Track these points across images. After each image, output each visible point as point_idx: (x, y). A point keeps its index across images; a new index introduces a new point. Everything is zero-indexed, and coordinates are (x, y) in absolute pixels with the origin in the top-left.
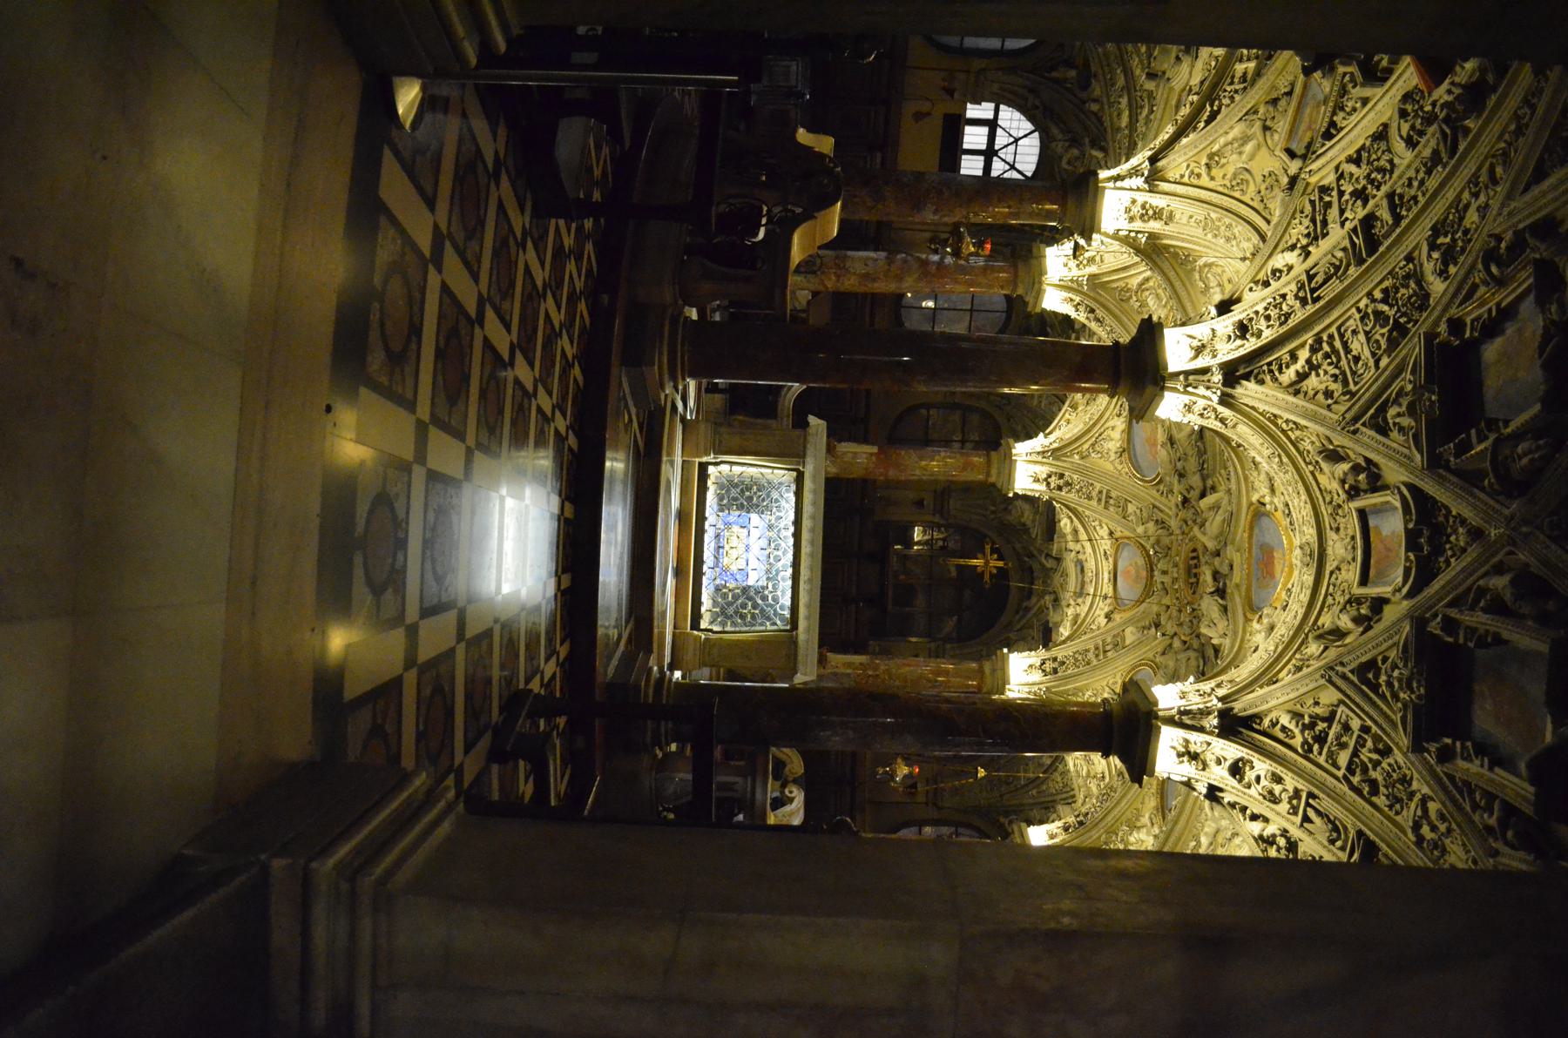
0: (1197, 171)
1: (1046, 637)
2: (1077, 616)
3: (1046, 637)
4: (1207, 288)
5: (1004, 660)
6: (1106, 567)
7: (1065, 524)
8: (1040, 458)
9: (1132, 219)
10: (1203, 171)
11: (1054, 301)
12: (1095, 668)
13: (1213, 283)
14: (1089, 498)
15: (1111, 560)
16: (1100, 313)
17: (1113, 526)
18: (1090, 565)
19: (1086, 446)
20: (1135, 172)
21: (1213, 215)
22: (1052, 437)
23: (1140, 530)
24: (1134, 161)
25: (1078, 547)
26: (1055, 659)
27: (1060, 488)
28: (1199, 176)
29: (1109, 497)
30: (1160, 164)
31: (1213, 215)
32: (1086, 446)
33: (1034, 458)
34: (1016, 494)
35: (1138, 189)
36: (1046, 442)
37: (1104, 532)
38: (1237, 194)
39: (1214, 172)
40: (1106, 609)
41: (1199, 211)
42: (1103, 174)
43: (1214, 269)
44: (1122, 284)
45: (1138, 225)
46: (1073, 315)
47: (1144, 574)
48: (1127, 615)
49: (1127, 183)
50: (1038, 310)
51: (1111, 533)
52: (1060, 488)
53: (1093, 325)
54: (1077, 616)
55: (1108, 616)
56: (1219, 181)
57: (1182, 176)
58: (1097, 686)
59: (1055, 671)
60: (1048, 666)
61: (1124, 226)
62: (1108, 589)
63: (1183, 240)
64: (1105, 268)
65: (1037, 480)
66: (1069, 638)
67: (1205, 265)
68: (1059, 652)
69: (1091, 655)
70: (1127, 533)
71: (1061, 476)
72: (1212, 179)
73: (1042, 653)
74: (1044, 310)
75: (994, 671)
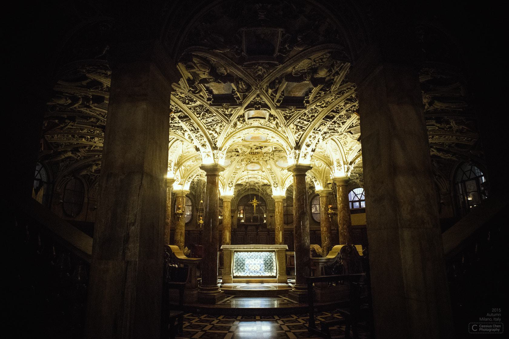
6: (251, 172)
11: (187, 188)
16: (190, 176)
23: (243, 165)
55: (263, 172)
62: (256, 172)
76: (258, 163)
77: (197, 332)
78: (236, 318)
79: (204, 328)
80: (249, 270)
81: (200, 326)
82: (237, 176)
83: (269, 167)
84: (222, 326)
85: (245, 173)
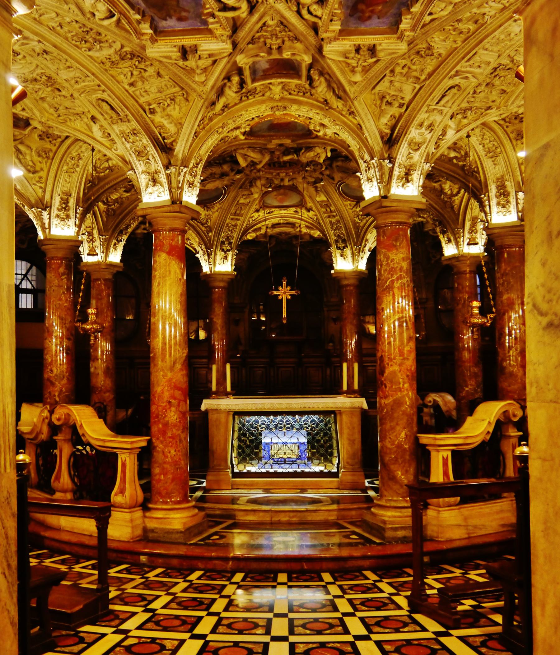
0: (37, 179)
1: (323, 244)
2: (307, 227)
3: (323, 244)
4: (109, 168)
5: (338, 272)
7: (250, 236)
8: (212, 256)
9: (68, 217)
10: (37, 175)
11: (115, 257)
12: (342, 217)
13: (106, 165)
14: (236, 225)
15: (273, 210)
16: (123, 227)
17: (252, 210)
18: (275, 221)
19: (203, 229)
20: (39, 217)
21: (65, 168)
22: (198, 248)
23: (256, 196)
24: (31, 216)
25: (264, 228)
26: (337, 241)
27: (230, 243)
28: (41, 178)
29: (235, 214)
30: (33, 201)
31: (65, 168)
32: (203, 229)
33: (212, 260)
34: (235, 270)
35: (50, 214)
36: (201, 252)
37: (256, 215)
38: (51, 155)
39: (38, 168)
40: (304, 211)
41: (63, 176)
42: (41, 236)
43: (98, 165)
44: (104, 215)
45: (72, 213)
46: (123, 243)
47: (282, 191)
48: (308, 199)
49: (46, 222)
50: (122, 265)
51: (257, 211)
52: (230, 243)
53: (130, 230)
54: (307, 227)
55: (309, 210)
56: (44, 165)
57: (41, 187)
58: (352, 215)
59: (344, 241)
60: (341, 245)
61: (71, 222)
62: (291, 210)
63: (80, 184)
64: (95, 226)
65: (226, 258)
66: (322, 231)
67: (96, 170)
68: (332, 238)
69: (333, 220)
70: (257, 202)
71: (223, 243)
72: (42, 169)
73: (333, 249)
74: (121, 261)
75: (345, 278)
76: (294, 189)
77: (134, 614)
78: (229, 579)
79: (151, 602)
80: (271, 457)
81: (142, 597)
82: (242, 223)
83: (322, 198)
84: (195, 599)
85: (261, 213)
